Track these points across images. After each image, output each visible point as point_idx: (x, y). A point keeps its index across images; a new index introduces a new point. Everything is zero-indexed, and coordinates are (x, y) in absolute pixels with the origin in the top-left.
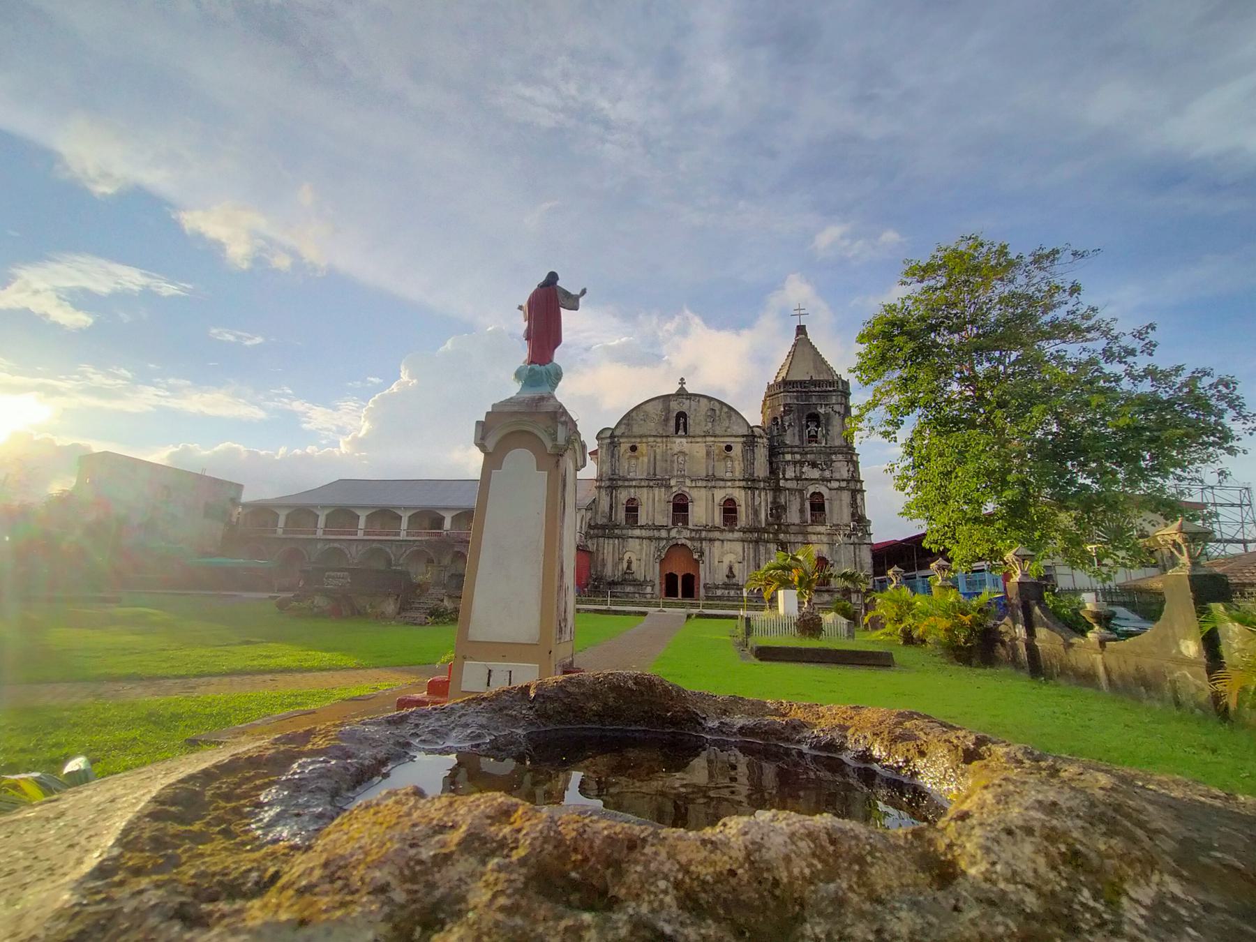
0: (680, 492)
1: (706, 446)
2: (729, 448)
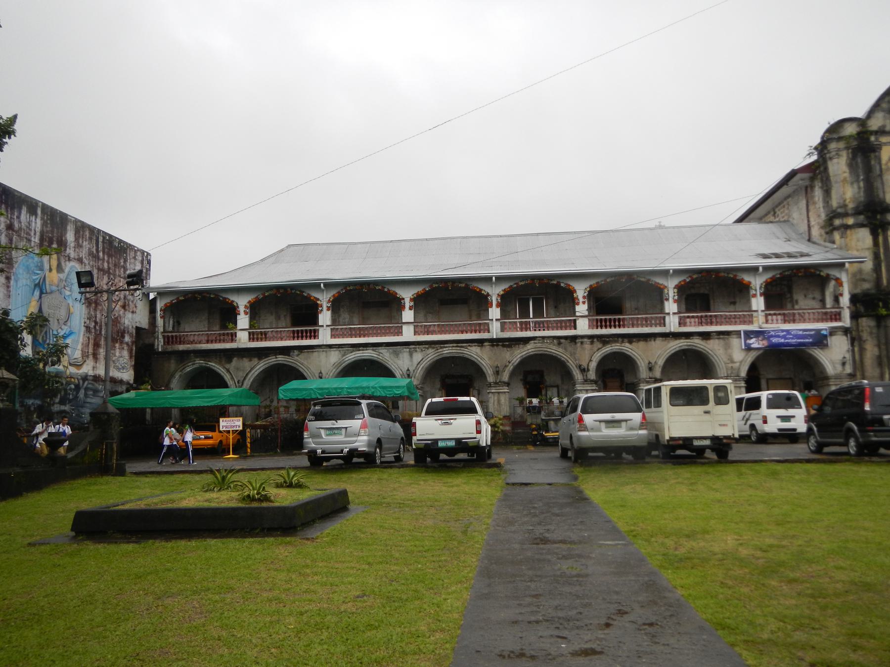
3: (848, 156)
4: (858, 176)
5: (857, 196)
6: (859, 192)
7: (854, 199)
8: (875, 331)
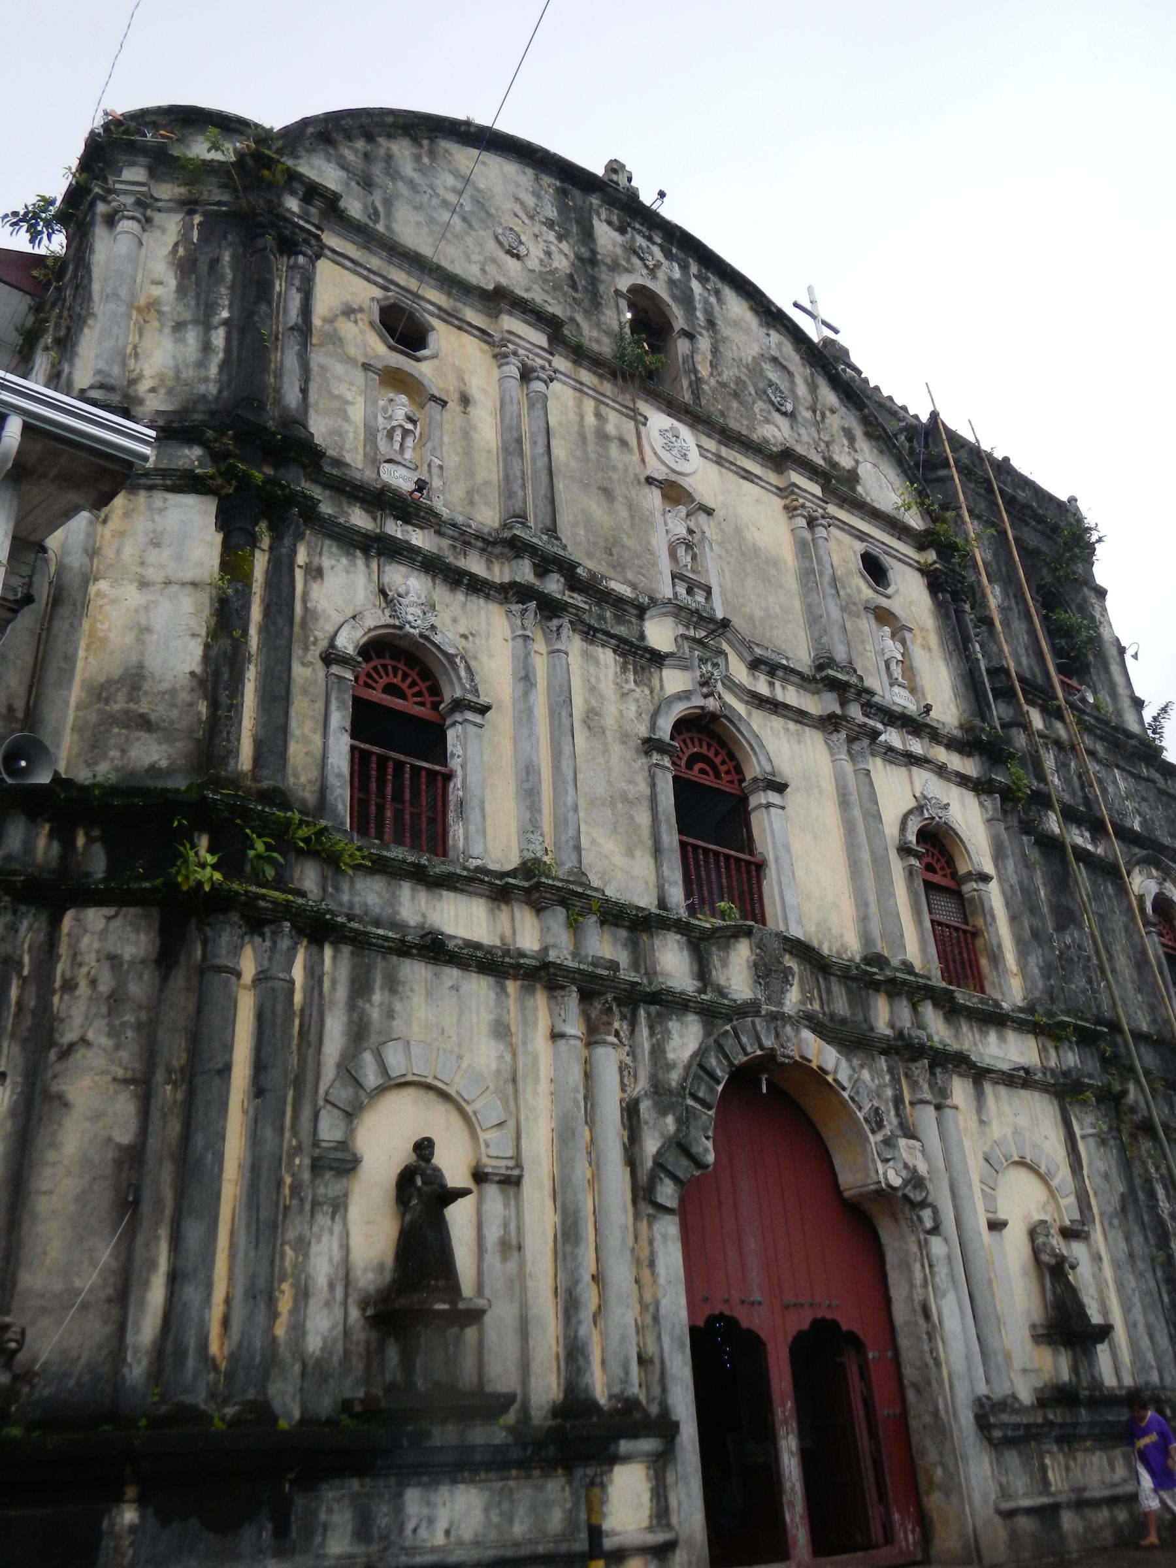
0: (711, 704)
1: (791, 510)
2: (874, 569)
3: (185, 237)
4: (209, 308)
5: (189, 373)
6: (201, 364)
7: (174, 382)
8: (137, 989)
